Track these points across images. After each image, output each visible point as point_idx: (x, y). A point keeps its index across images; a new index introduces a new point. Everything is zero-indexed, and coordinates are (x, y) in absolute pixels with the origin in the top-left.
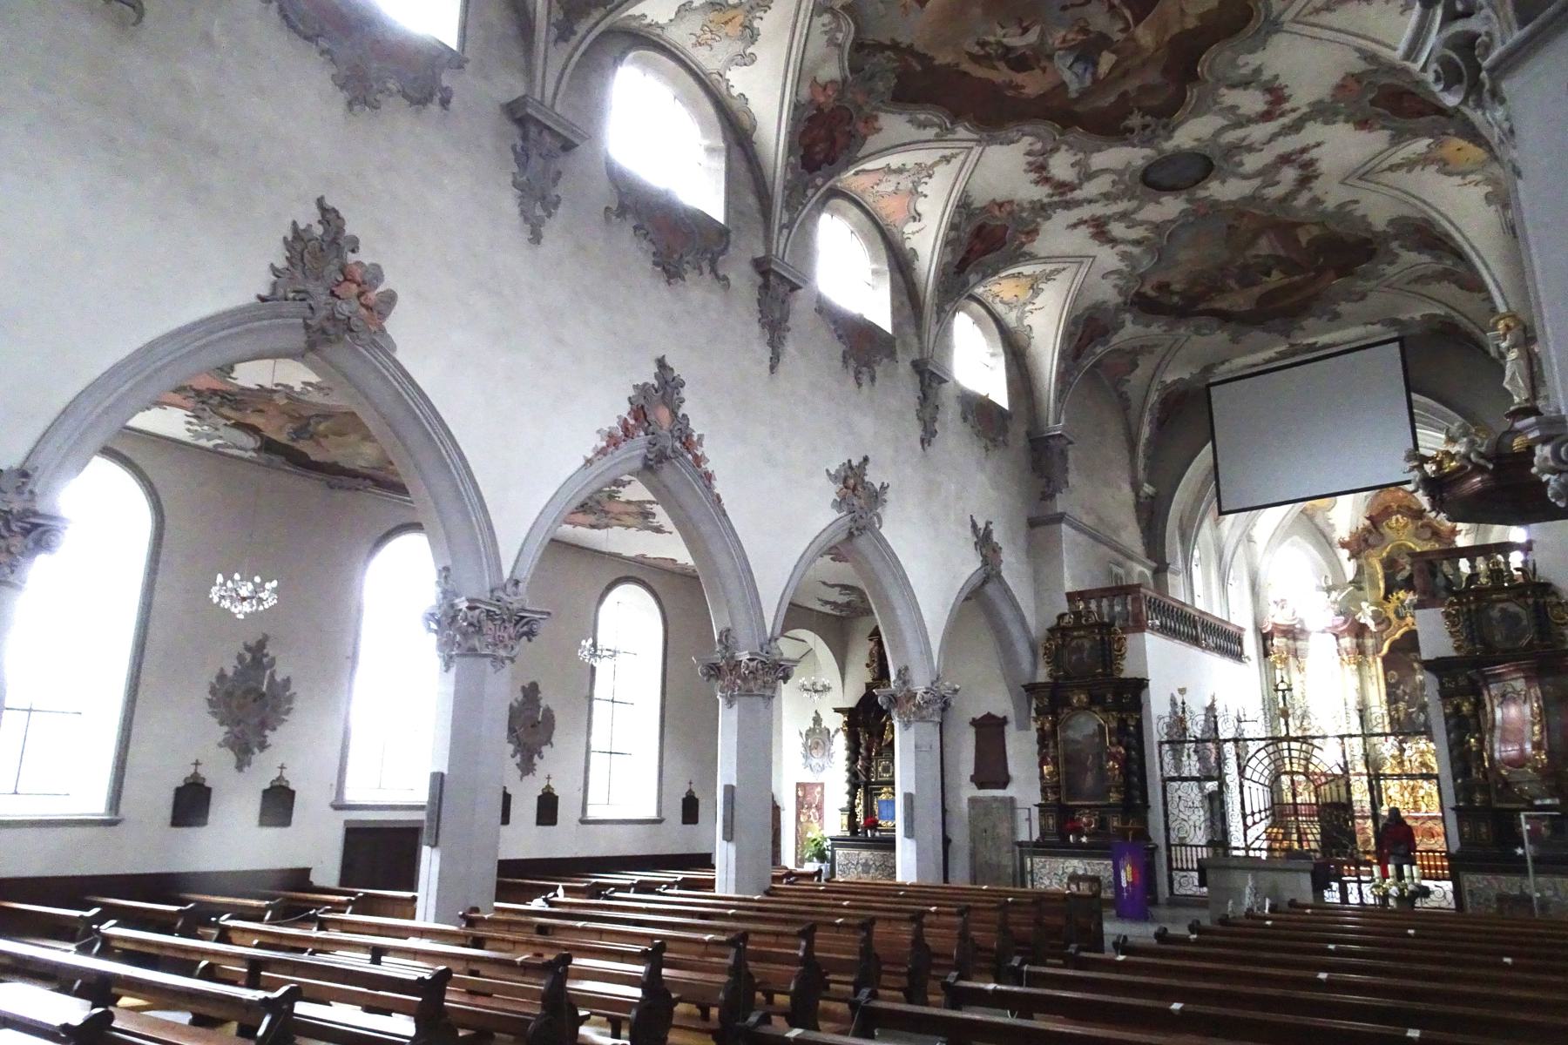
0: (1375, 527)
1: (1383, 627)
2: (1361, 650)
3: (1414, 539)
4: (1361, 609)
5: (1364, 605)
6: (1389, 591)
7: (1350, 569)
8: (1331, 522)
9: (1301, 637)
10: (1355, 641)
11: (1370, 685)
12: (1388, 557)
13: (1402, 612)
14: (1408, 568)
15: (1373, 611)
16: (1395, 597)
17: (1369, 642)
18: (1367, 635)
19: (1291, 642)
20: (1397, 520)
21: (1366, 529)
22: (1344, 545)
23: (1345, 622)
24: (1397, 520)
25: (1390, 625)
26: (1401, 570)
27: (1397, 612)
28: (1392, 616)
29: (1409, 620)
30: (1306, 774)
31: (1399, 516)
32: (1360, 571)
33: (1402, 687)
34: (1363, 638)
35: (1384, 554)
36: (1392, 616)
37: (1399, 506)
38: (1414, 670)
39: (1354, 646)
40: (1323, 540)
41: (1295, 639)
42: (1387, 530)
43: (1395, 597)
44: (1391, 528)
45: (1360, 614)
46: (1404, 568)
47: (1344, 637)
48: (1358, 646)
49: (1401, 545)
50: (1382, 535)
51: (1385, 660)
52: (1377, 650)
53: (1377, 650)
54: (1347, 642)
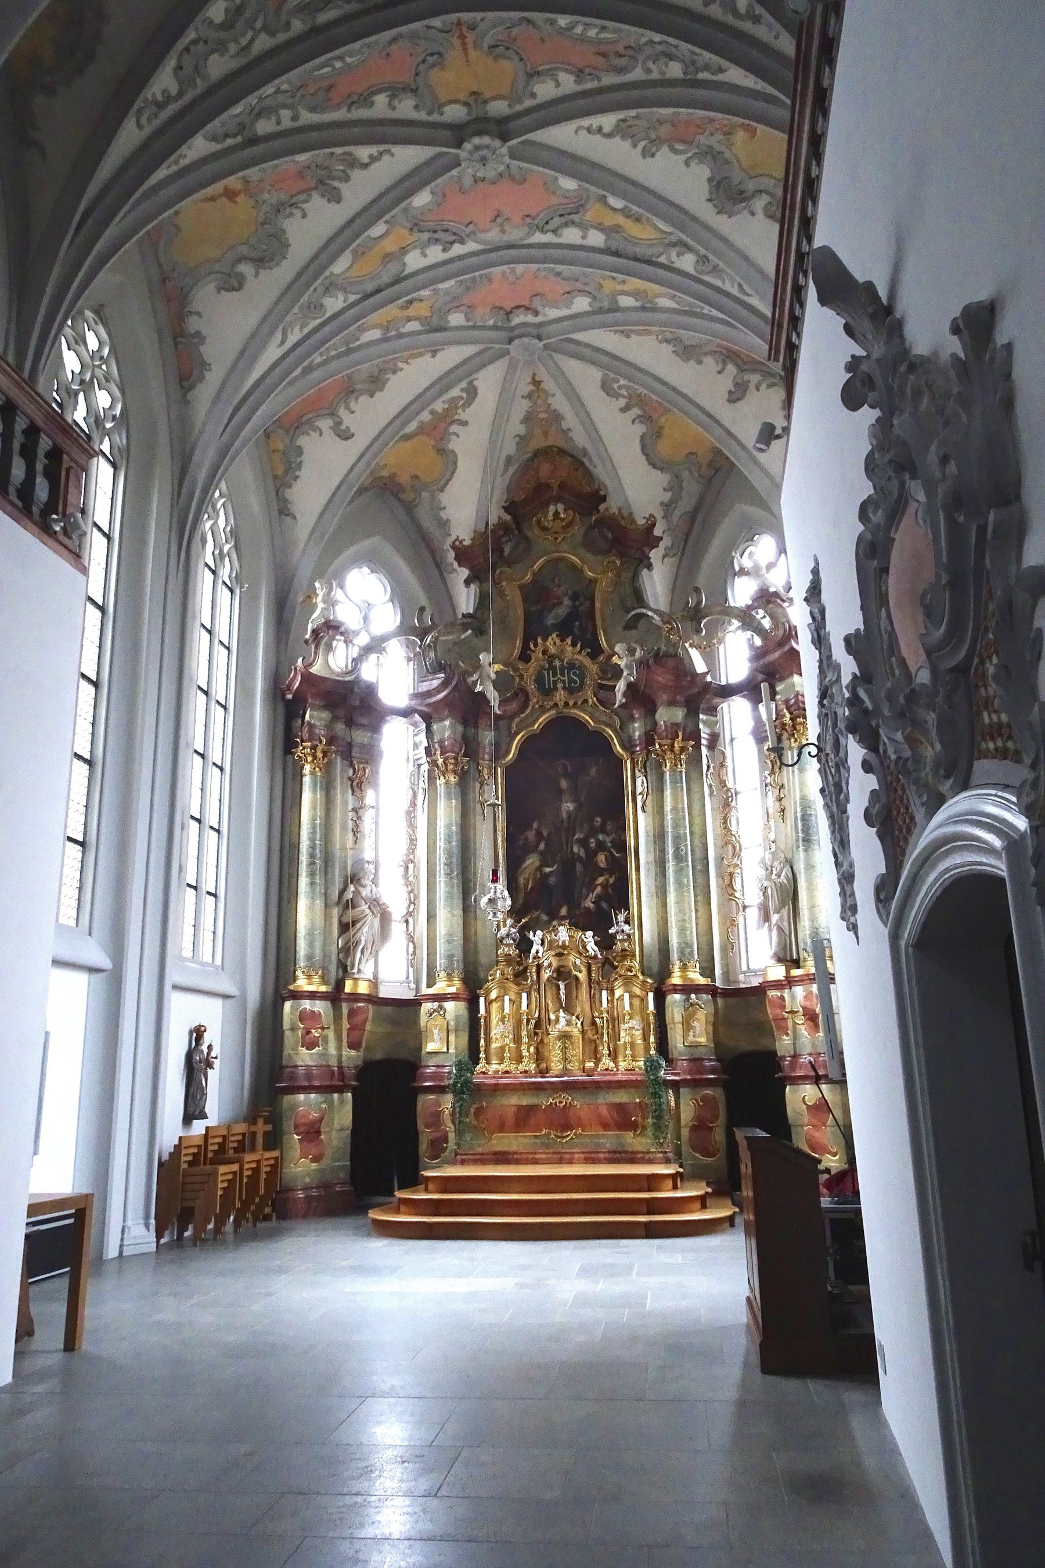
0: (519, 528)
1: (514, 706)
2: (469, 747)
3: (582, 552)
4: (477, 666)
5: (484, 658)
6: (529, 637)
7: (466, 600)
8: (444, 515)
9: (363, 721)
10: (460, 728)
11: (479, 818)
12: (534, 582)
13: (549, 678)
14: (566, 602)
15: (497, 673)
16: (540, 648)
17: (488, 737)
18: (483, 722)
19: (340, 727)
20: (556, 514)
21: (501, 525)
22: (463, 555)
23: (445, 684)
24: (556, 514)
25: (527, 699)
26: (554, 606)
27: (539, 681)
28: (531, 687)
29: (560, 696)
30: (336, 996)
31: (560, 507)
32: (482, 601)
33: (535, 825)
34: (476, 727)
35: (528, 577)
36: (531, 687)
37: (561, 486)
38: (560, 792)
39: (459, 737)
40: (426, 554)
41: (350, 723)
42: (537, 531)
43: (540, 648)
44: (545, 529)
45: (475, 677)
46: (561, 603)
47: (441, 720)
48: (465, 738)
49: (559, 560)
50: (527, 539)
51: (509, 771)
52: (499, 752)
53: (499, 752)
54: (446, 728)
